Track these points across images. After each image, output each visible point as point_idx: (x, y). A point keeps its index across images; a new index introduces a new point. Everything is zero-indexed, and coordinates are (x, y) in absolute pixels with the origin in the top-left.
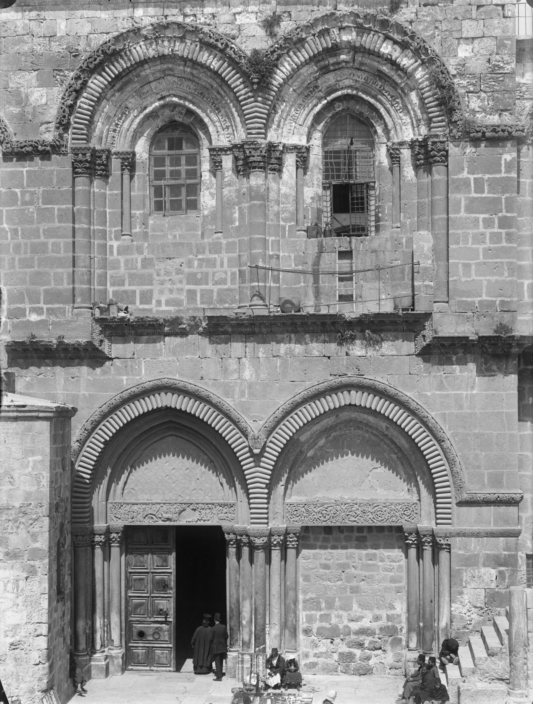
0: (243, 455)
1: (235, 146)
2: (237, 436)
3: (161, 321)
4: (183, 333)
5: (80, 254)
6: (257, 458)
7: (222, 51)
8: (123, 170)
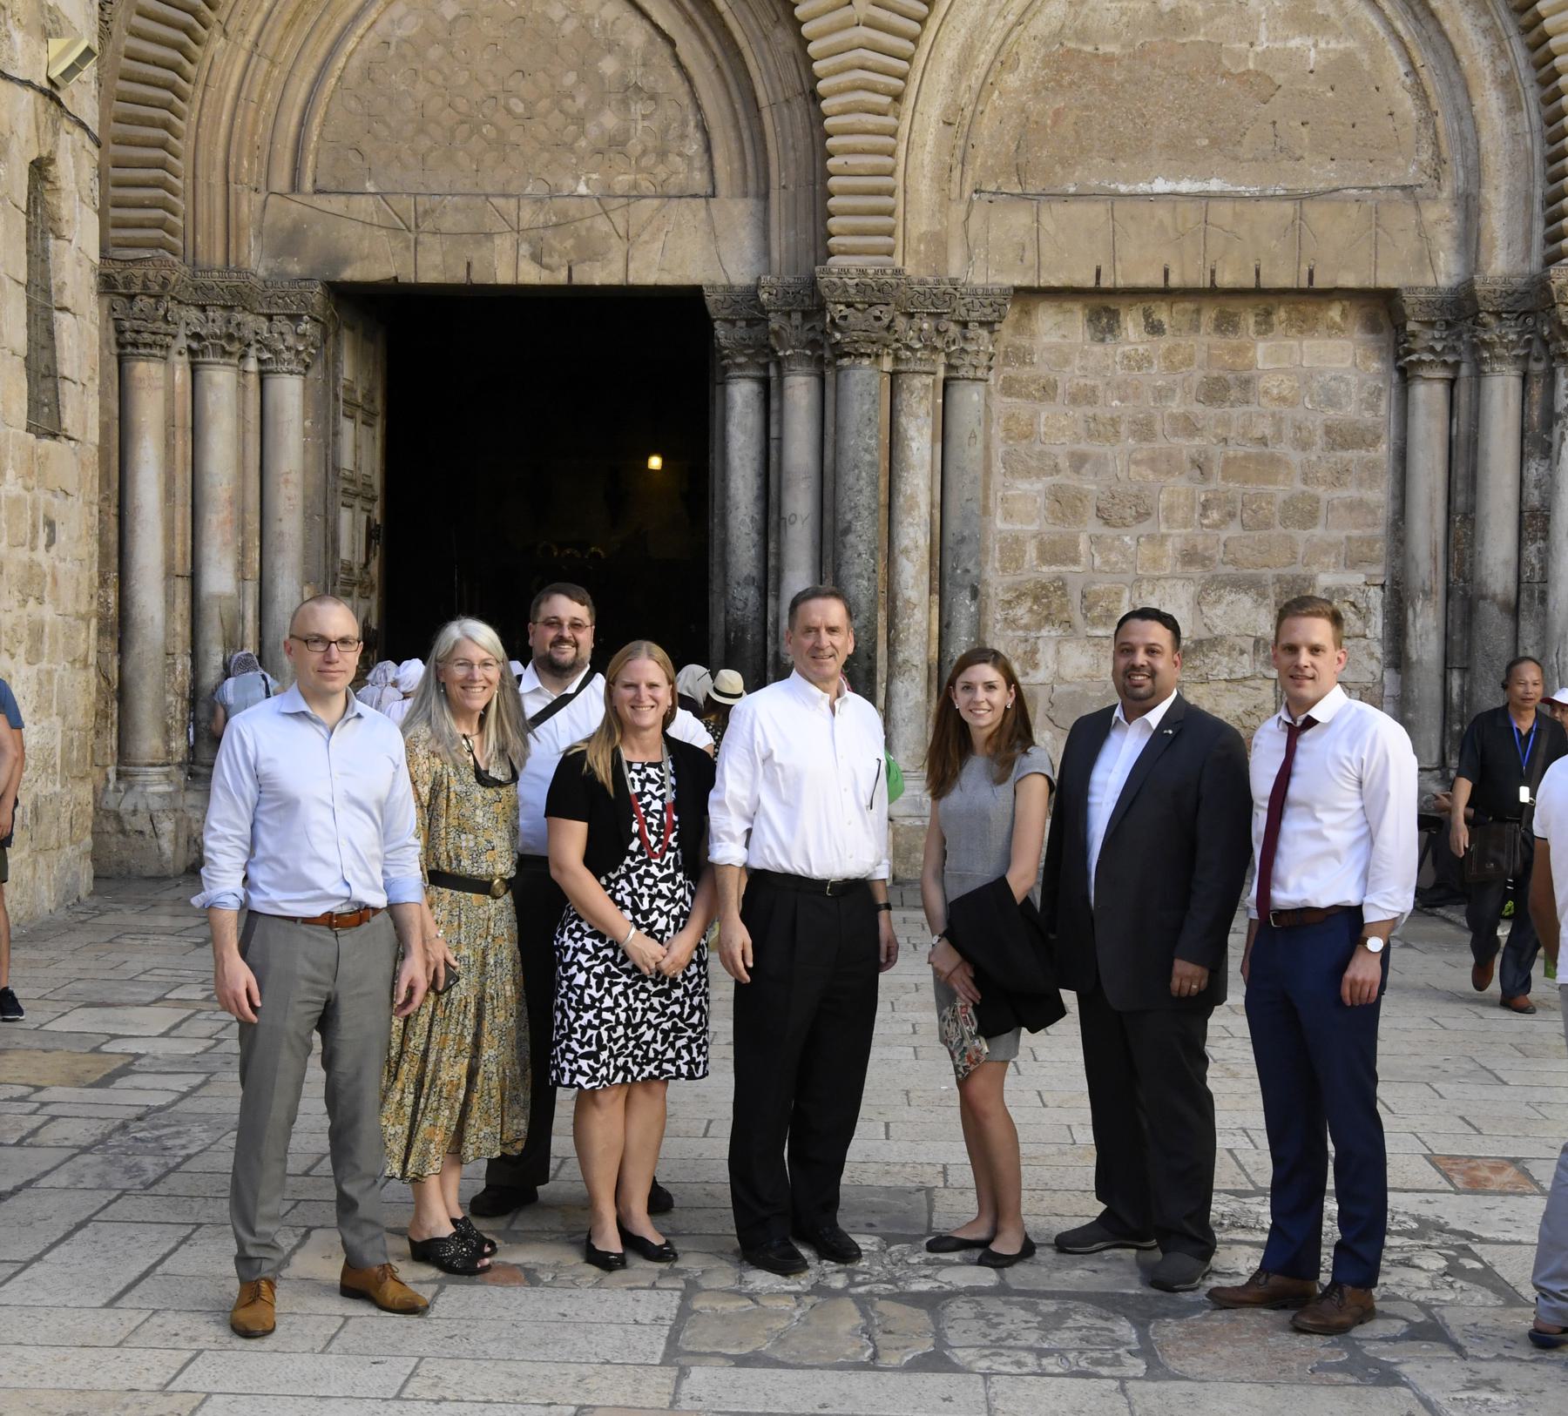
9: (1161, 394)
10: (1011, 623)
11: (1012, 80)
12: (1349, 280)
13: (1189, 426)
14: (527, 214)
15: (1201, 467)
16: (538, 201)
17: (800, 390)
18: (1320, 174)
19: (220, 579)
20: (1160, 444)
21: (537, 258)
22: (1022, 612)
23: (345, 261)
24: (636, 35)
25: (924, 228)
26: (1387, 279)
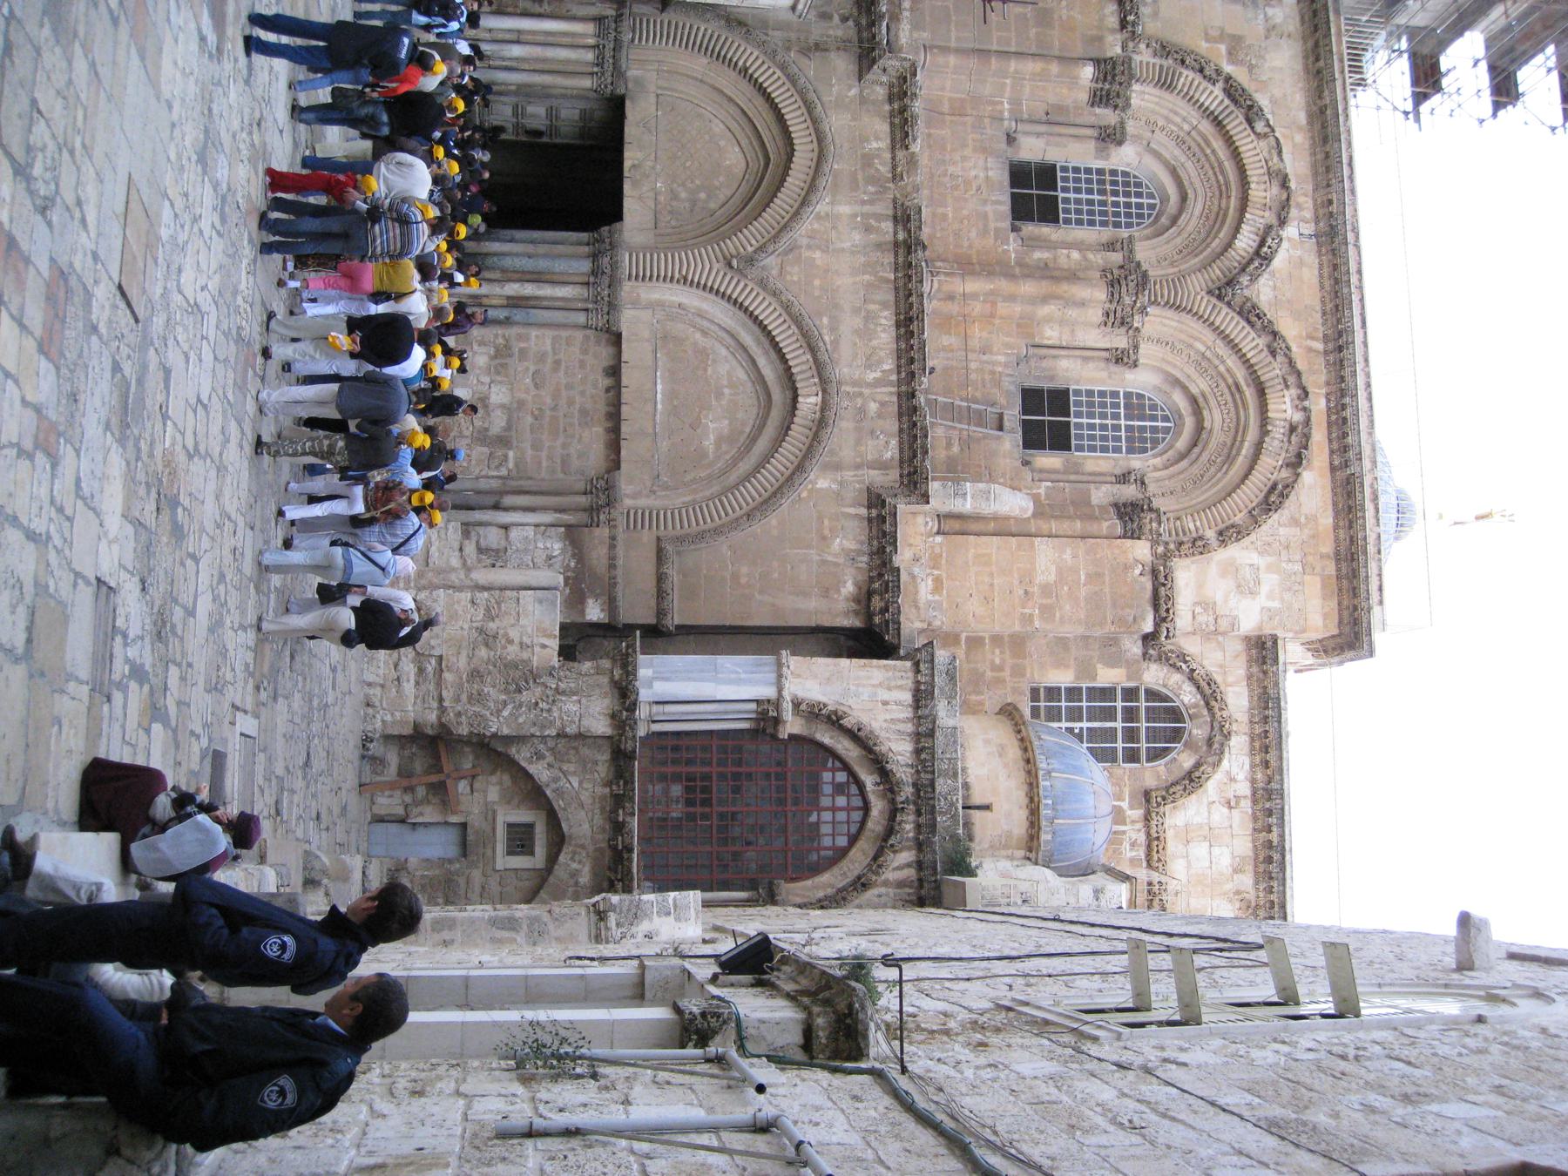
1: (1139, 265)
7: (1257, 253)
9: (582, 393)
10: (496, 336)
11: (698, 335)
12: (623, 453)
13: (571, 403)
14: (650, 164)
15: (554, 409)
16: (653, 168)
17: (586, 249)
18: (664, 445)
19: (516, 51)
20: (564, 393)
21: (634, 166)
22: (501, 341)
23: (632, 99)
24: (713, 205)
25: (643, 296)
26: (623, 465)
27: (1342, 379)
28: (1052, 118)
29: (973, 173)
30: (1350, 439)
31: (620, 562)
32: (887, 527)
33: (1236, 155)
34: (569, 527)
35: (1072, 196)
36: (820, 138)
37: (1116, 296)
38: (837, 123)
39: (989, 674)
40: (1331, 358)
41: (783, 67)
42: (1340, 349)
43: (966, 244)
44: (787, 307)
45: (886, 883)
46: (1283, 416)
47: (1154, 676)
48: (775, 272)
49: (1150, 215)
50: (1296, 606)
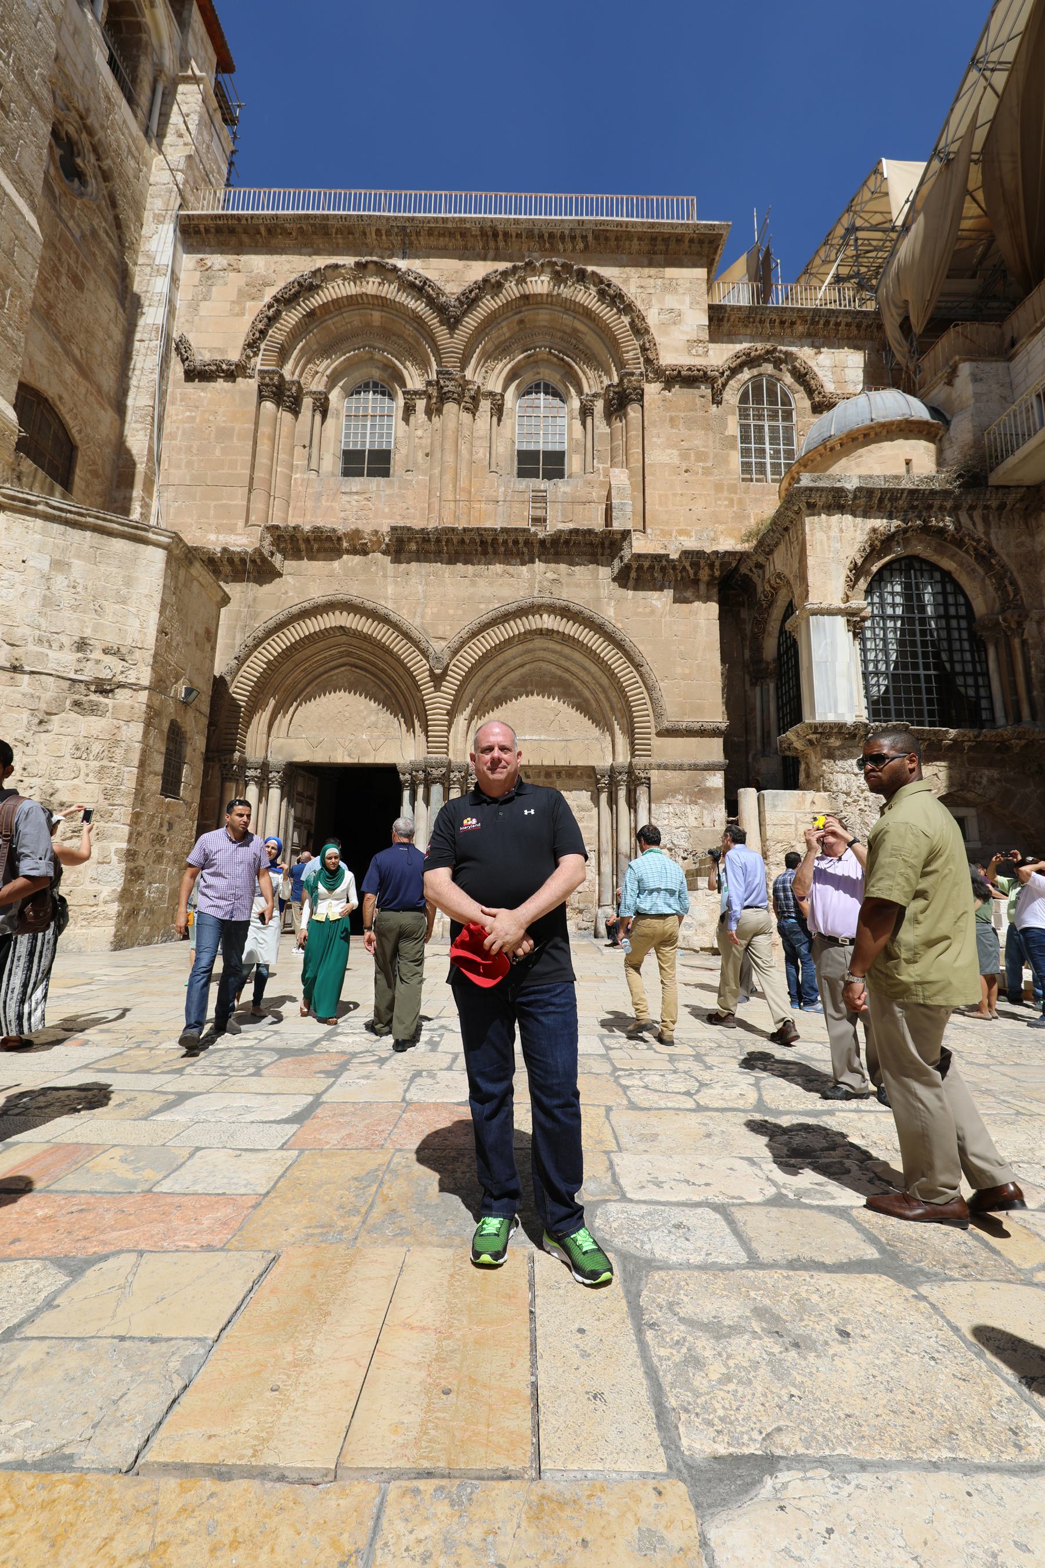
0: (423, 677)
2: (418, 658)
3: (340, 533)
4: (364, 552)
5: (260, 474)
6: (437, 680)
8: (314, 410)
21: (349, 755)
27: (519, 236)
28: (307, 445)
29: (354, 503)
30: (567, 232)
31: (679, 761)
32: (646, 564)
33: (338, 305)
34: (650, 802)
35: (368, 440)
36: (330, 607)
37: (456, 396)
38: (317, 593)
39: (735, 509)
40: (501, 244)
41: (270, 633)
42: (495, 235)
43: (412, 511)
44: (474, 634)
45: (987, 534)
46: (546, 284)
47: (731, 396)
48: (444, 644)
49: (382, 387)
50: (688, 285)
